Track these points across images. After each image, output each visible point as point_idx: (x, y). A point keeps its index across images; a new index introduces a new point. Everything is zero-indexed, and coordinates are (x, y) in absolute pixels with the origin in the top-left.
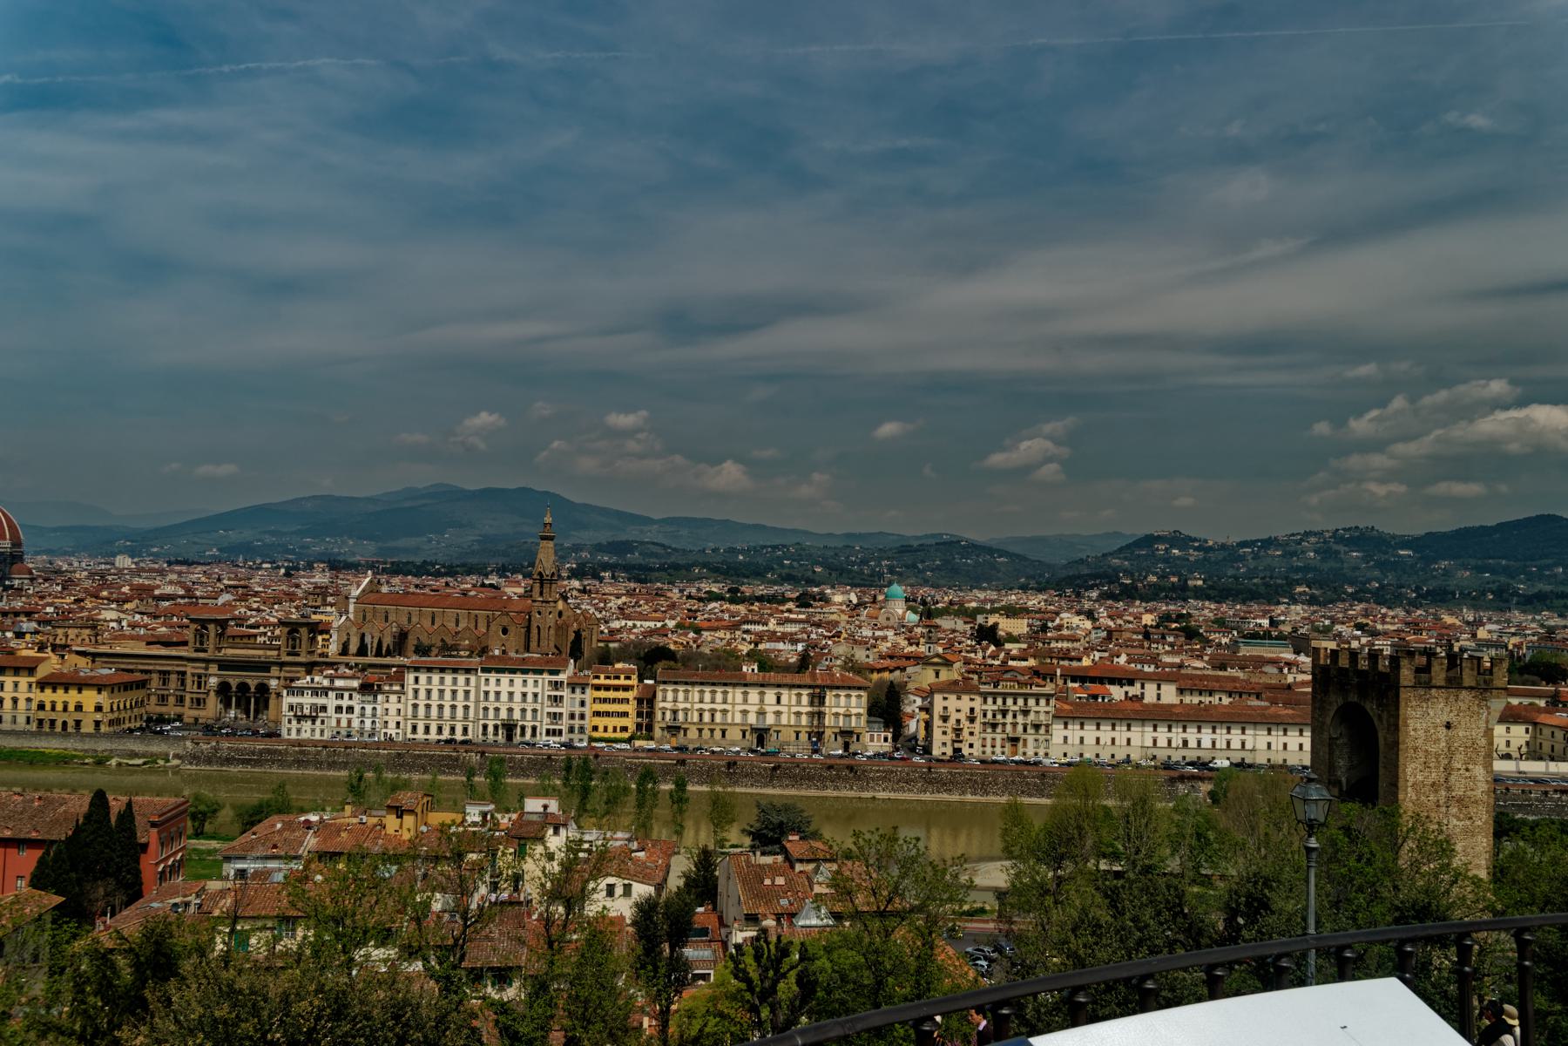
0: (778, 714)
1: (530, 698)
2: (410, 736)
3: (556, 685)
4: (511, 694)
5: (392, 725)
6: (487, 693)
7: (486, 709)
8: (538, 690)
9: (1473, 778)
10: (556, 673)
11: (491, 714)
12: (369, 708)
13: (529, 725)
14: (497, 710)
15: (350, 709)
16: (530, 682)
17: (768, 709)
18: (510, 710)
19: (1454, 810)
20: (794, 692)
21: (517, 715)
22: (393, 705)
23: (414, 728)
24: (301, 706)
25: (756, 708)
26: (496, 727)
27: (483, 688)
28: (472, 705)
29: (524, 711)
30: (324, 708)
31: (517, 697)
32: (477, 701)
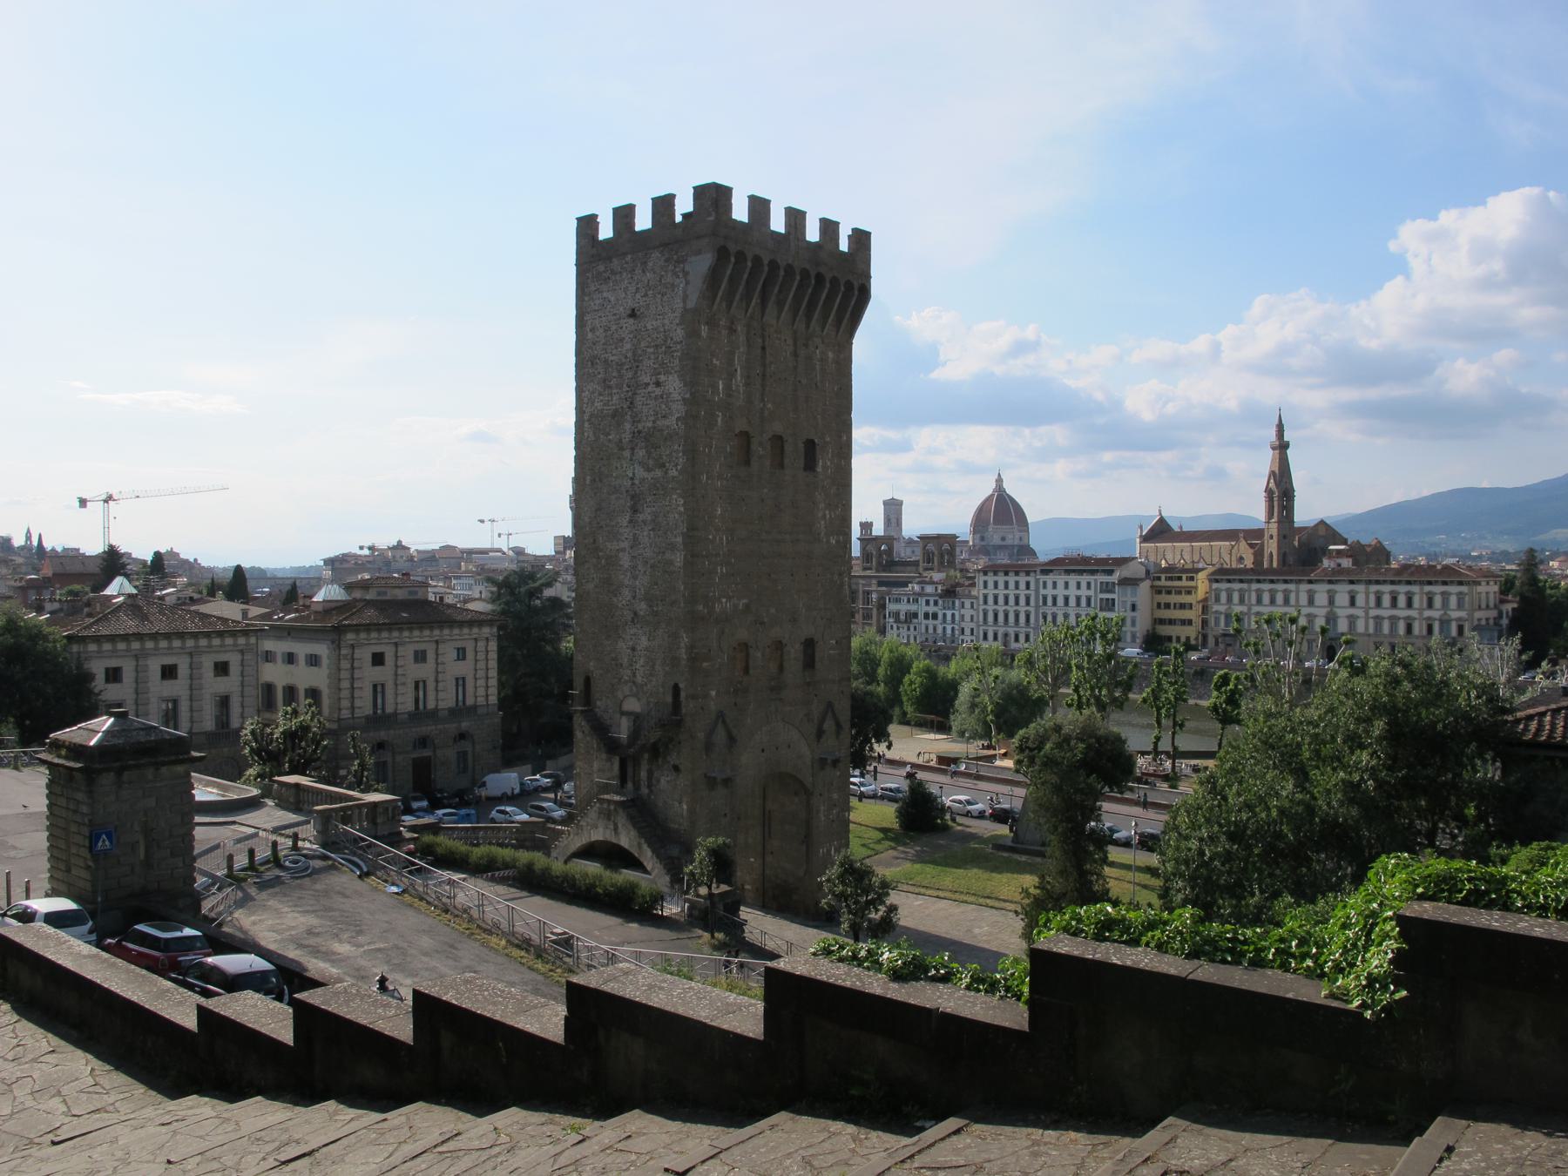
0: (1352, 620)
3: (1107, 588)
4: (1066, 599)
5: (967, 631)
8: (1091, 593)
9: (664, 398)
12: (949, 613)
15: (935, 616)
16: (1084, 585)
17: (1340, 612)
18: (1066, 616)
19: (641, 453)
20: (1374, 588)
22: (968, 612)
25: (1323, 612)
27: (1042, 592)
28: (1032, 609)
30: (915, 615)
31: (1072, 602)
32: (1037, 607)
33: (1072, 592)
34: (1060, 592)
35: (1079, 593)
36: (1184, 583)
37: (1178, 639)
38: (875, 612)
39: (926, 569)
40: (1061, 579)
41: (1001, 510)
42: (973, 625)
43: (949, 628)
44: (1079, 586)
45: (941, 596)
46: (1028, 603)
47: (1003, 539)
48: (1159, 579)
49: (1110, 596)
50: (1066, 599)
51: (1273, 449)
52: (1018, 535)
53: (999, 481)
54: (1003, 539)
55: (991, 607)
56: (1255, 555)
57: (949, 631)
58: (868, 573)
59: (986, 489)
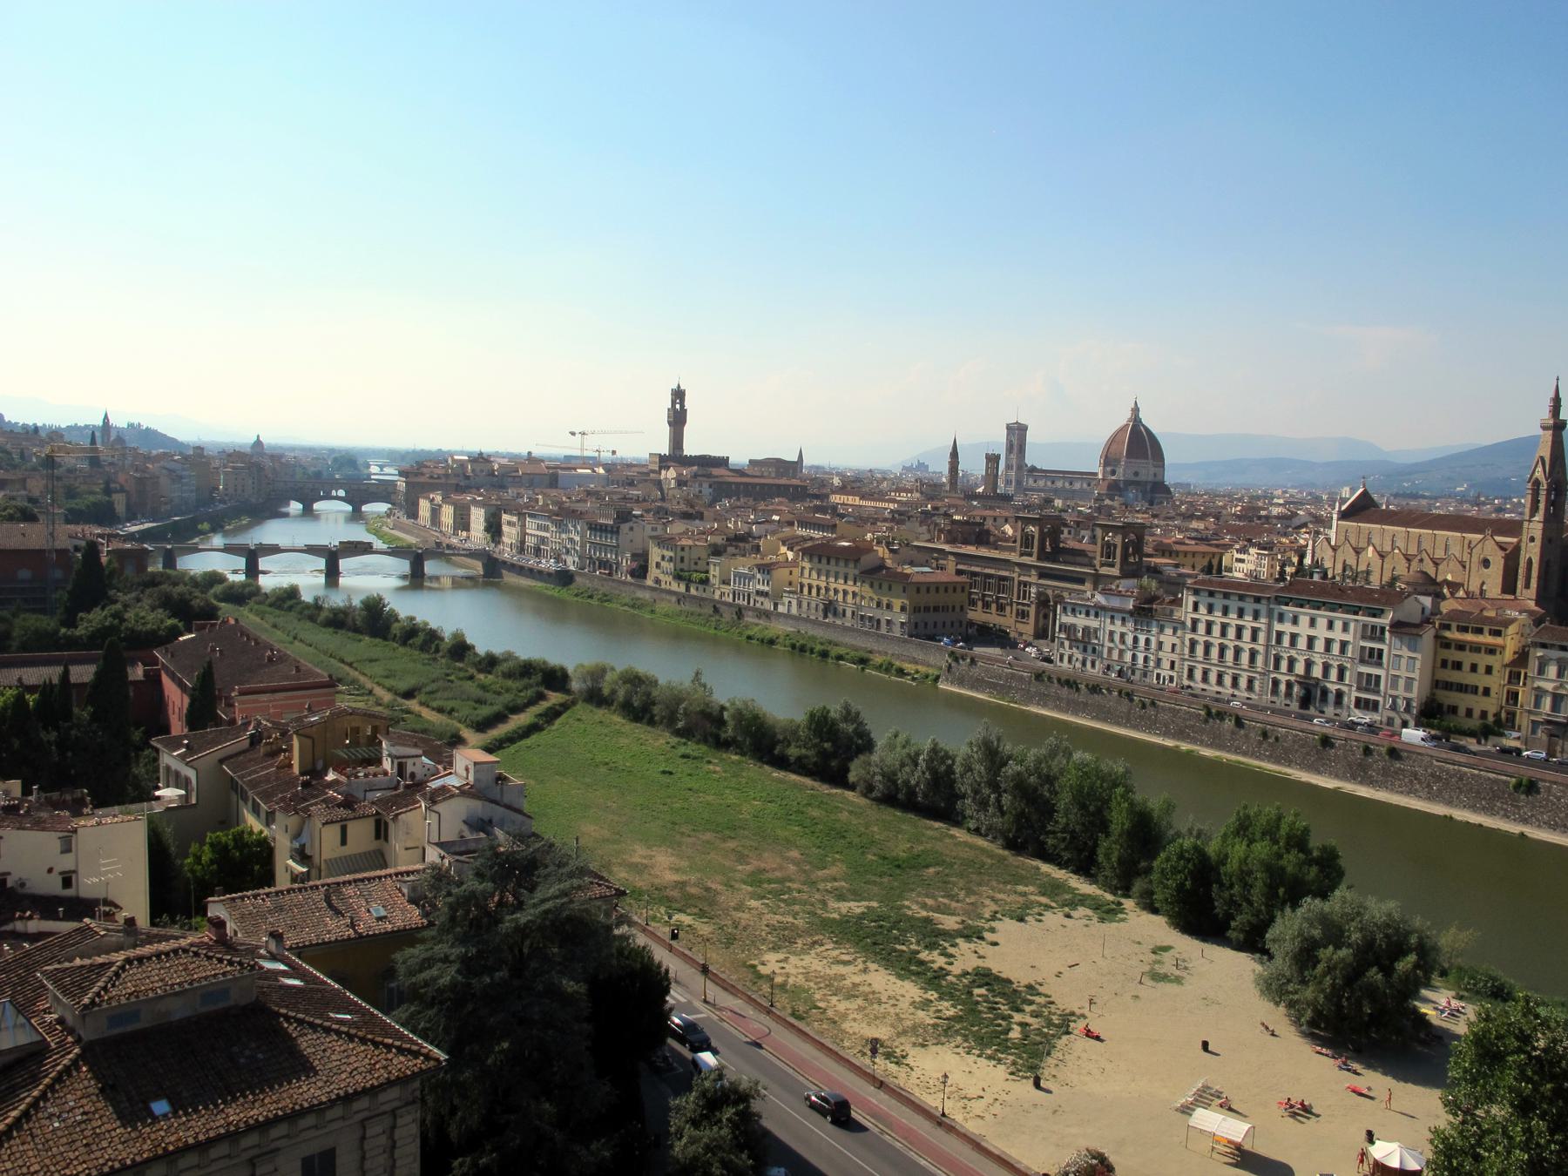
1: (1336, 648)
2: (1186, 682)
3: (1376, 633)
4: (1311, 640)
5: (1166, 664)
6: (1280, 635)
7: (1278, 659)
8: (1348, 637)
10: (1375, 614)
11: (1284, 665)
12: (1142, 639)
13: (1333, 688)
14: (1292, 661)
16: (1338, 625)
18: (1309, 664)
21: (1317, 672)
23: (1191, 676)
24: (1074, 626)
26: (1289, 685)
28: (1261, 649)
29: (1326, 668)
31: (1319, 646)
32: (1267, 646)
33: (1321, 632)
34: (1303, 629)
35: (1330, 635)
36: (1486, 639)
37: (1469, 713)
38: (1032, 610)
39: (1102, 565)
40: (1304, 615)
41: (1139, 442)
42: (1175, 657)
43: (1141, 657)
44: (1330, 626)
45: (1131, 613)
46: (1254, 638)
47: (1136, 474)
48: (1448, 627)
49: (1376, 646)
50: (1311, 640)
51: (1544, 428)
52: (1152, 470)
53: (1136, 410)
54: (1136, 474)
55: (1201, 637)
56: (1507, 558)
57: (1140, 661)
58: (1026, 560)
59: (1122, 418)
